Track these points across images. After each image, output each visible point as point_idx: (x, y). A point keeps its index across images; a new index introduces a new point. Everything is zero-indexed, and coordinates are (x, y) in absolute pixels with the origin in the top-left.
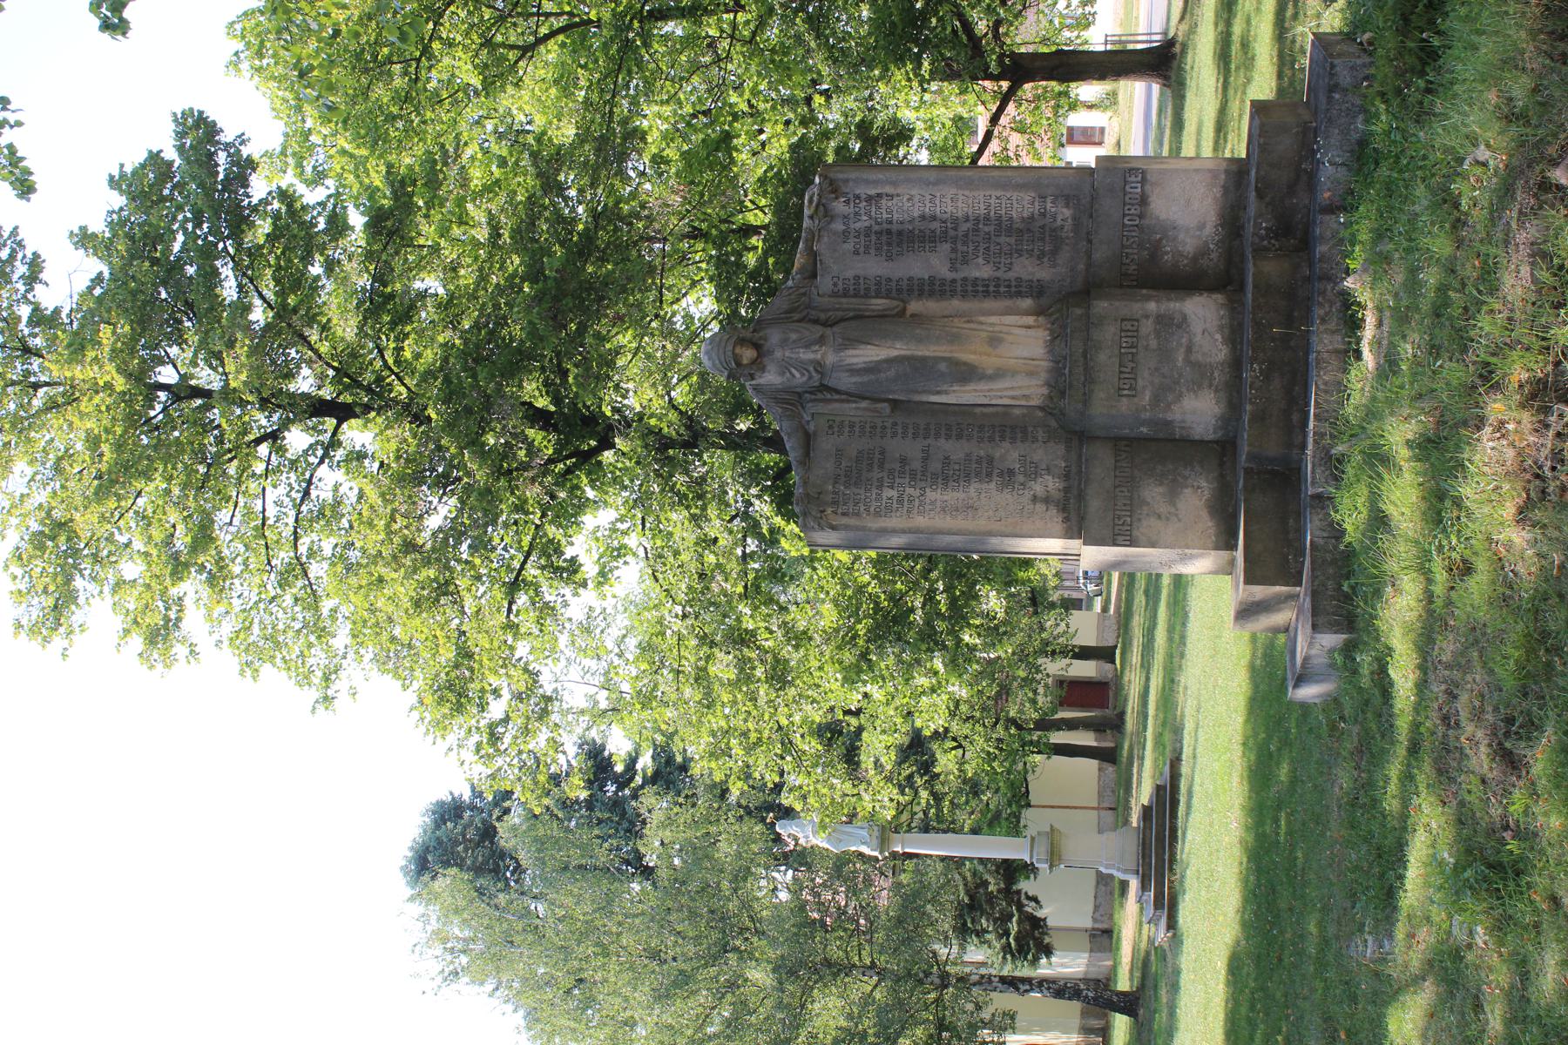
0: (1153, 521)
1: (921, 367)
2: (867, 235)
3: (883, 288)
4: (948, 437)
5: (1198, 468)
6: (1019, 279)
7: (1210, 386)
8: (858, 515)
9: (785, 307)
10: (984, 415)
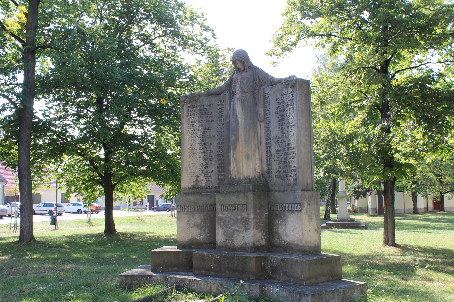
0: (187, 219)
3: (267, 111)
4: (219, 144)
8: (188, 115)
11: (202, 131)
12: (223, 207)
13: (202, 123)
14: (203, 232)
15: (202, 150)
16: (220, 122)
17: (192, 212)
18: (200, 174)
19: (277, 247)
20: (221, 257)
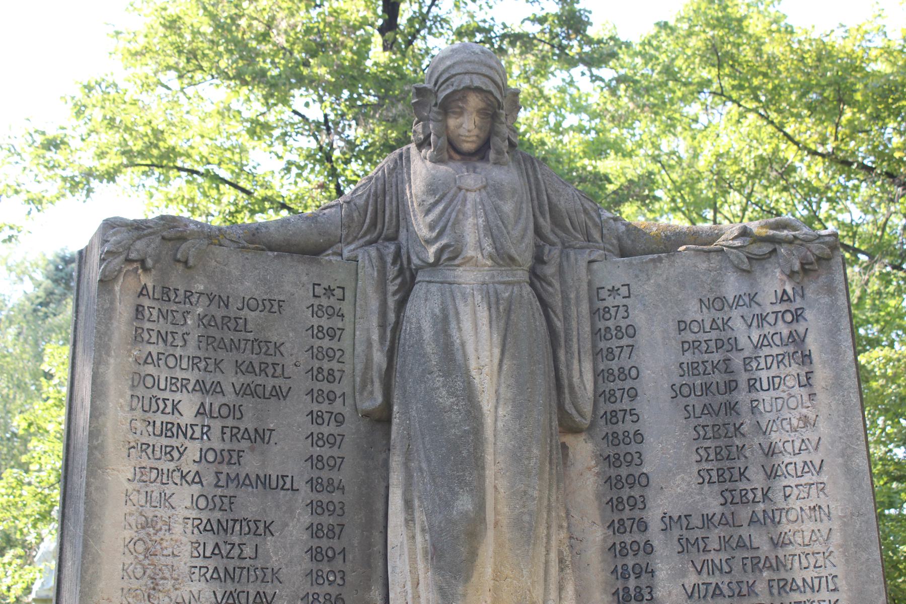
1: (461, 457)
2: (720, 344)
4: (314, 531)
8: (137, 338)
9: (563, 204)
11: (218, 445)
13: (221, 400)
15: (211, 564)
16: (325, 407)
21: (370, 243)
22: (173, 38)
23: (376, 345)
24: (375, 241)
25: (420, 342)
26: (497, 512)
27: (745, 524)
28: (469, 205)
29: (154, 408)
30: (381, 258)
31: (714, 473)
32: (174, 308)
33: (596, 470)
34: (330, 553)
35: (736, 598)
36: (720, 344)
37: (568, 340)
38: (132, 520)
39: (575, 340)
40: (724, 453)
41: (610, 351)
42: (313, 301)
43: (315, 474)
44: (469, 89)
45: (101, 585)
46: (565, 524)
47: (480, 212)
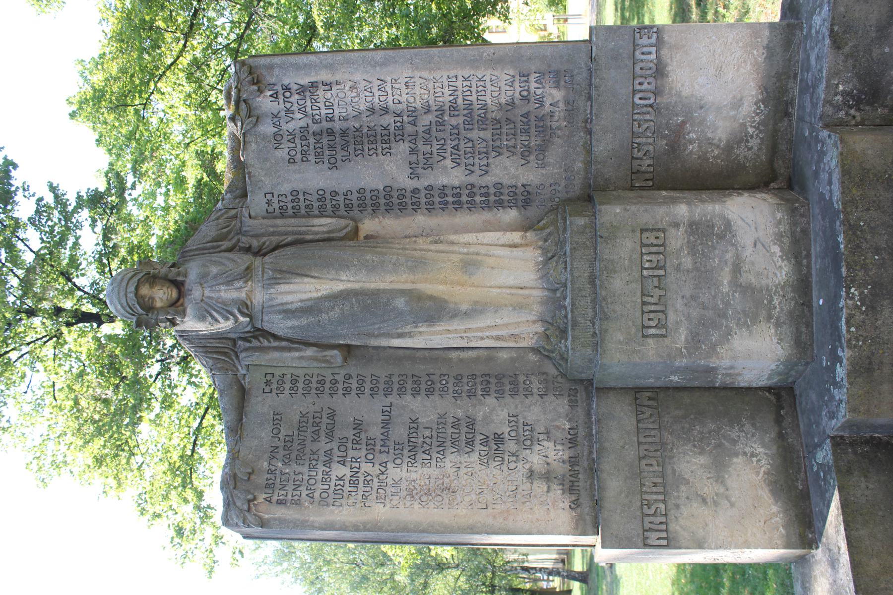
1: (371, 303)
2: (304, 138)
3: (326, 203)
4: (416, 393)
5: (748, 427)
6: (499, 185)
7: (769, 317)
8: (297, 503)
10: (461, 360)
11: (363, 452)
12: (652, 331)
13: (336, 451)
14: (739, 447)
15: (435, 455)
16: (340, 386)
17: (666, 485)
18: (520, 465)
19: (774, 150)
20: (853, 281)
21: (237, 357)
22: (108, 460)
23: (302, 354)
24: (236, 353)
25: (300, 328)
26: (406, 282)
27: (416, 128)
28: (213, 295)
29: (340, 492)
30: (247, 349)
31: (384, 146)
32: (278, 480)
33: (381, 218)
34: (429, 383)
35: (460, 137)
36: (303, 138)
37: (300, 233)
38: (408, 504)
39: (300, 229)
40: (372, 139)
41: (307, 207)
42: (274, 393)
43: (381, 392)
44: (136, 295)
45: (446, 521)
46: (414, 239)
47: (217, 288)
